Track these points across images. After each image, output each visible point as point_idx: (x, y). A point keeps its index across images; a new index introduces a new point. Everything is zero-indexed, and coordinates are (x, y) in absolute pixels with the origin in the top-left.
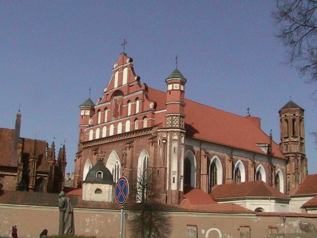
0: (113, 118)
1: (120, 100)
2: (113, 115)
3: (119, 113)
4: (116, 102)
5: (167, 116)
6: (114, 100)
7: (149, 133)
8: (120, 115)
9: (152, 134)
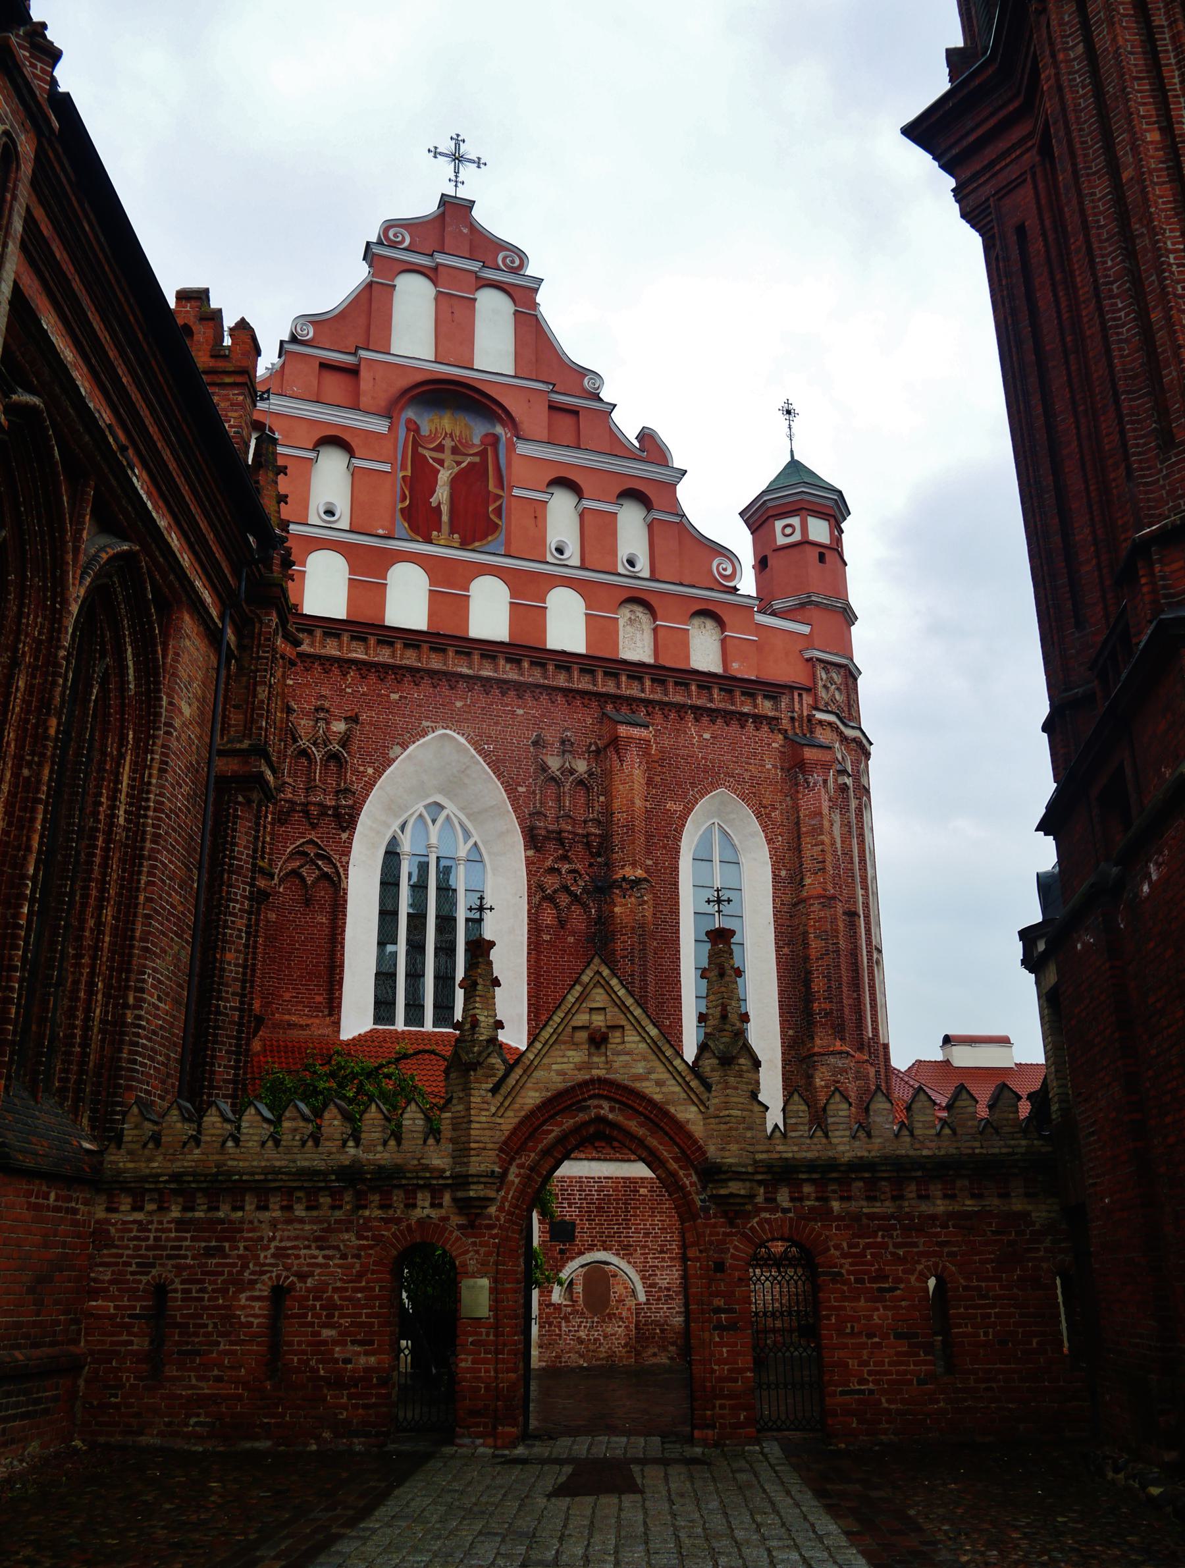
0: (402, 527)
1: (448, 443)
2: (400, 506)
3: (445, 518)
4: (416, 444)
5: (818, 660)
6: (409, 421)
7: (766, 707)
8: (452, 532)
9: (785, 724)
